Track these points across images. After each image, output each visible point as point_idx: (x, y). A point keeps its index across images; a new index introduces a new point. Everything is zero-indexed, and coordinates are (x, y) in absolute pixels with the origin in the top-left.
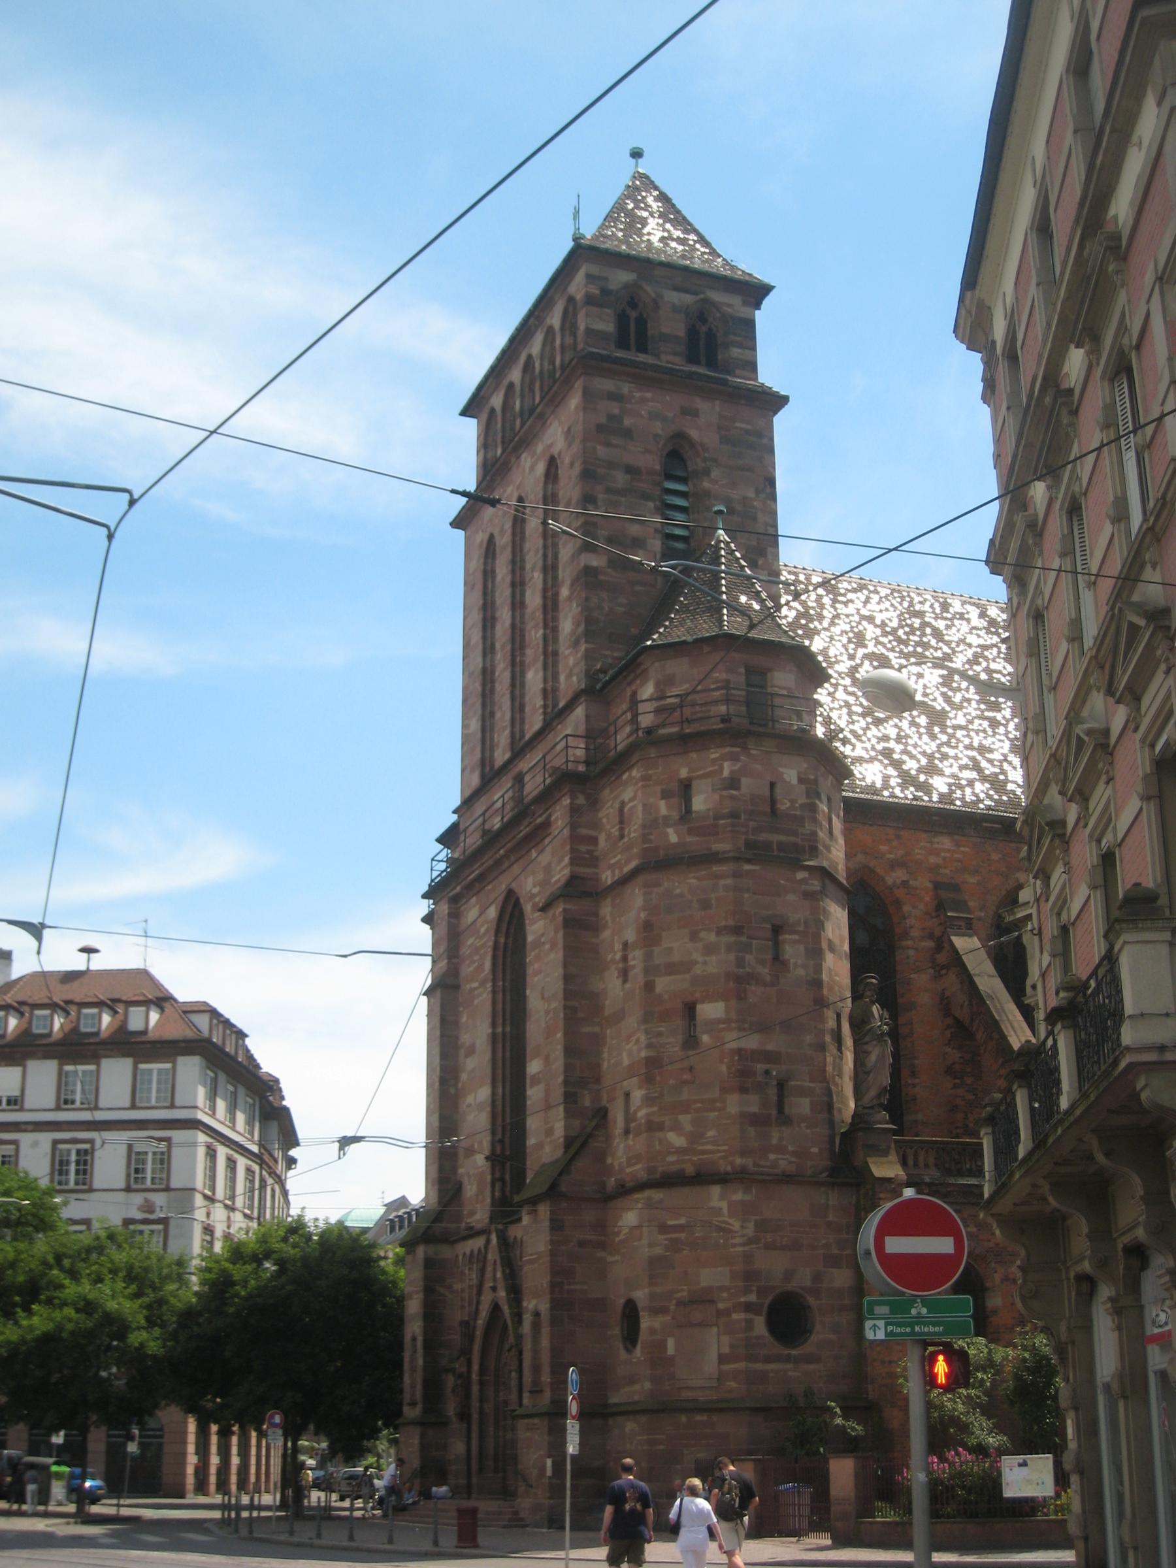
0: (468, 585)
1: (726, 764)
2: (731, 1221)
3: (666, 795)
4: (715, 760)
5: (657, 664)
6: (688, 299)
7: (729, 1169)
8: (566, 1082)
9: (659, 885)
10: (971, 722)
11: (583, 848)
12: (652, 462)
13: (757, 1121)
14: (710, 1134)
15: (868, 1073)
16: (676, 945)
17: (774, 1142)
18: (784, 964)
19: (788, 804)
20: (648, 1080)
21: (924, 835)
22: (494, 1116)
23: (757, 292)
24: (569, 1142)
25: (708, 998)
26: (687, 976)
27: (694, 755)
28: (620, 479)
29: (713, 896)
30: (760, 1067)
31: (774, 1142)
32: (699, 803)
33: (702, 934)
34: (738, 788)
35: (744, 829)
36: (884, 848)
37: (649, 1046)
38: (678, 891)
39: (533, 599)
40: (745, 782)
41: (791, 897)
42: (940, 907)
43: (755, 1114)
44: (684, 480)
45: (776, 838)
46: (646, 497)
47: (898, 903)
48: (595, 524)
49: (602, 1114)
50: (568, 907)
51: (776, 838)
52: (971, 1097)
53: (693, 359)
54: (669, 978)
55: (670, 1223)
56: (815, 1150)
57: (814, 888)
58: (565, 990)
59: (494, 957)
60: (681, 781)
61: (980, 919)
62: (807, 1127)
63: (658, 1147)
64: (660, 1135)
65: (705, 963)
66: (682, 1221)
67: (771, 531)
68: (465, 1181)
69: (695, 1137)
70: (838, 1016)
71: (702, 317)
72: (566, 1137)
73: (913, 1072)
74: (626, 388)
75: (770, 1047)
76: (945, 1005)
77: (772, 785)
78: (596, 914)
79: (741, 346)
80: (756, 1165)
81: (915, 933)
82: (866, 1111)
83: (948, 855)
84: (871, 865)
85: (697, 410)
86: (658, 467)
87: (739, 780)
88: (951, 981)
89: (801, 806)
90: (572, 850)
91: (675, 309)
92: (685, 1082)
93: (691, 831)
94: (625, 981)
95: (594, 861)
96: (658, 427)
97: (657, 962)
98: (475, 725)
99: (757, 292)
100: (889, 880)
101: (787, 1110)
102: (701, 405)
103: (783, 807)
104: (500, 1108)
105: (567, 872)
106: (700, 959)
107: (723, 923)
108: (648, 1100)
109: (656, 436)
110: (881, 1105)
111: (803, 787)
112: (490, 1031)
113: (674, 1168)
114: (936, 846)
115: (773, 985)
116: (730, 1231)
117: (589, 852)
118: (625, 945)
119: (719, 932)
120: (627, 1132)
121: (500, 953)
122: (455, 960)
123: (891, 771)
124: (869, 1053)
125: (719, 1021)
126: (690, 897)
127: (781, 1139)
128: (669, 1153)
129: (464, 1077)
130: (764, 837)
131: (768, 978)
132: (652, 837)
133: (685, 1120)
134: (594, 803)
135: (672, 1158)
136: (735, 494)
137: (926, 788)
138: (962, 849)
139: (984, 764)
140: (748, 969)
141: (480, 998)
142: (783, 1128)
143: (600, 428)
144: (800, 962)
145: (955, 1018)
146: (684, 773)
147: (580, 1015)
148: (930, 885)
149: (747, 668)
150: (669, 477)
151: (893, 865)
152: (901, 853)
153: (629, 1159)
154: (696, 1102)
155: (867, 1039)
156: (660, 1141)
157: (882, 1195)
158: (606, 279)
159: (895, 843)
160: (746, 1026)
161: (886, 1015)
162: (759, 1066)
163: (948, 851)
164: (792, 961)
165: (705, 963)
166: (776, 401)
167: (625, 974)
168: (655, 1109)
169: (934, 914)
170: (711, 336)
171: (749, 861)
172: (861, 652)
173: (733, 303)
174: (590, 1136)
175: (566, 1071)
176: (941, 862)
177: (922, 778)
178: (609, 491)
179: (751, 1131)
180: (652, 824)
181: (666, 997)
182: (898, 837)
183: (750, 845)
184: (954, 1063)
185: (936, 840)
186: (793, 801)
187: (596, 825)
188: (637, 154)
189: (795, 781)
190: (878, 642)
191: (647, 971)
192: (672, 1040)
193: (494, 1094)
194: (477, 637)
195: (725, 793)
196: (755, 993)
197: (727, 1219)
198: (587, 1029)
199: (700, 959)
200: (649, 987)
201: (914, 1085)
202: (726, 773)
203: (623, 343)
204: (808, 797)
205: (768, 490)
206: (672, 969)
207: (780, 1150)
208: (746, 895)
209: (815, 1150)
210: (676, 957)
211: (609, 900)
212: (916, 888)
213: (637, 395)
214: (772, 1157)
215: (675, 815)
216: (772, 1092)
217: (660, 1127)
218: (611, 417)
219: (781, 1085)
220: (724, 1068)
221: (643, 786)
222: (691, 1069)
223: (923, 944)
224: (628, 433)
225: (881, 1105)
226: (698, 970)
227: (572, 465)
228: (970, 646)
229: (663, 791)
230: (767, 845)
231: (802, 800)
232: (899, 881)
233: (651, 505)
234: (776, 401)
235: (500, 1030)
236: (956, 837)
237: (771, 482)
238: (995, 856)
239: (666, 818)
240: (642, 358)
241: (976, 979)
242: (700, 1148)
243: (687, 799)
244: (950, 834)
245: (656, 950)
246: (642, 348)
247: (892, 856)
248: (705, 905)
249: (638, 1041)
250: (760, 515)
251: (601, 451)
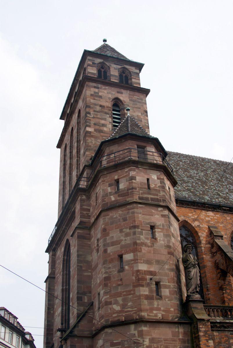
0: (61, 161)
1: (130, 172)
2: (139, 339)
3: (110, 185)
4: (126, 172)
5: (107, 148)
6: (120, 67)
7: (137, 317)
8: (78, 293)
9: (108, 215)
10: (215, 185)
11: (85, 213)
12: (109, 104)
13: (148, 297)
14: (129, 304)
15: (191, 279)
16: (115, 235)
17: (155, 306)
18: (156, 239)
19: (154, 186)
20: (106, 285)
21: (203, 211)
22: (62, 317)
23: (140, 66)
24: (78, 315)
25: (127, 252)
26: (119, 245)
27: (120, 171)
28: (98, 108)
29: (128, 216)
30: (148, 277)
31: (155, 306)
32: (122, 186)
33: (124, 230)
34: (136, 180)
35: (138, 193)
36: (190, 215)
37: (106, 273)
38: (115, 216)
39: (75, 151)
40: (138, 178)
41: (157, 216)
42: (211, 233)
43: (147, 295)
44: (119, 111)
45: (150, 196)
46: (106, 113)
47: (196, 233)
48: (90, 120)
49: (92, 304)
50: (79, 231)
51: (150, 196)
52: (229, 297)
54: (112, 247)
55: (115, 342)
56: (172, 309)
57: (165, 214)
58: (78, 260)
59: (63, 263)
60: (115, 180)
61: (225, 238)
62: (169, 300)
63: (109, 311)
64: (110, 306)
65: (126, 240)
66: (120, 340)
67: (147, 124)
68: (55, 343)
69: (124, 306)
70: (178, 261)
72: (77, 313)
73: (208, 290)
74: (100, 86)
75: (152, 269)
76: (216, 265)
77: (148, 180)
78: (90, 234)
79: (135, 79)
80: (148, 315)
81: (204, 242)
82: (191, 294)
83: (212, 217)
84: (187, 220)
85: (122, 92)
86: (110, 106)
87: (136, 177)
88: (218, 257)
89: (159, 186)
90: (81, 213)
91: (115, 69)
92: (119, 285)
93: (119, 196)
94: (98, 253)
95: (89, 217)
96: (110, 96)
97: (108, 242)
98: (61, 198)
99: (140, 66)
100: (193, 225)
101: (159, 294)
103: (152, 187)
104: (64, 315)
105: (79, 221)
106: (124, 239)
107: (132, 225)
108: (105, 293)
109: (109, 98)
110: (197, 292)
111: (159, 181)
112: (62, 288)
113: (116, 319)
114: (208, 214)
115: (152, 247)
116: (139, 343)
117: (86, 214)
118: (98, 240)
119: (130, 229)
120: (99, 308)
121: (65, 262)
122: (54, 269)
123: (191, 194)
124: (191, 272)
125: (132, 260)
126: (119, 218)
127: (158, 305)
128: (115, 313)
129: (55, 306)
130: (145, 196)
131: (150, 244)
132: (105, 200)
133: (120, 299)
134: (89, 198)
135: (114, 315)
137: (203, 198)
138: (217, 216)
139: (221, 194)
140: (141, 241)
141: (59, 278)
142: (159, 301)
143: (92, 95)
144: (161, 239)
145: (221, 270)
146: (116, 177)
147: (83, 269)
148: (207, 227)
149: (137, 145)
150: (114, 110)
151: (195, 220)
152: (196, 216)
153: (100, 318)
154: (123, 292)
155: (189, 266)
156: (110, 309)
157: (201, 326)
158: (94, 60)
159: (194, 213)
160: (142, 261)
161: (196, 258)
162: (147, 276)
163: (212, 216)
164: (158, 238)
165: (126, 240)
166: (146, 92)
167: (98, 251)
168: (108, 296)
169: (209, 236)
170: (126, 77)
171: (140, 203)
172: (178, 167)
173: (133, 69)
174: (86, 312)
175: (78, 289)
176: (210, 220)
177: (201, 196)
178: (94, 111)
179: (146, 302)
180: (106, 195)
181: (111, 254)
182: (195, 211)
183: (140, 198)
184: (222, 285)
185: (208, 213)
186: (156, 185)
187: (89, 205)
188: (105, 41)
189: (156, 178)
190: (183, 166)
191: (104, 245)
192: (114, 269)
193: (62, 309)
194: (62, 174)
195: (131, 181)
196: (144, 249)
197: (137, 338)
198: (86, 274)
199: (124, 239)
200: (105, 251)
201: (208, 294)
202: (131, 175)
204: (161, 183)
205: (145, 114)
206: (113, 244)
207: (158, 309)
208: (140, 215)
209: (172, 309)
210: (115, 239)
211: (93, 228)
212: (202, 228)
213: (104, 87)
214: (155, 312)
215: (114, 191)
216: (154, 287)
217: (110, 303)
218: (95, 92)
219: (157, 284)
220: (134, 278)
221: (103, 184)
222: (121, 280)
223: (207, 246)
224: (101, 97)
225: (197, 292)
226: (123, 243)
227: (84, 107)
228: (212, 168)
229: (109, 184)
230: (147, 199)
231: (159, 185)
232: (196, 225)
233: (108, 115)
234: (146, 92)
235: (65, 287)
236: (215, 212)
237: (146, 112)
238: (228, 218)
239: (110, 193)
241: (227, 253)
242: (126, 310)
243: (118, 187)
244: (212, 211)
245: (108, 238)
247: (193, 217)
248: (125, 220)
249: (102, 272)
250: (143, 120)
251: (92, 101)
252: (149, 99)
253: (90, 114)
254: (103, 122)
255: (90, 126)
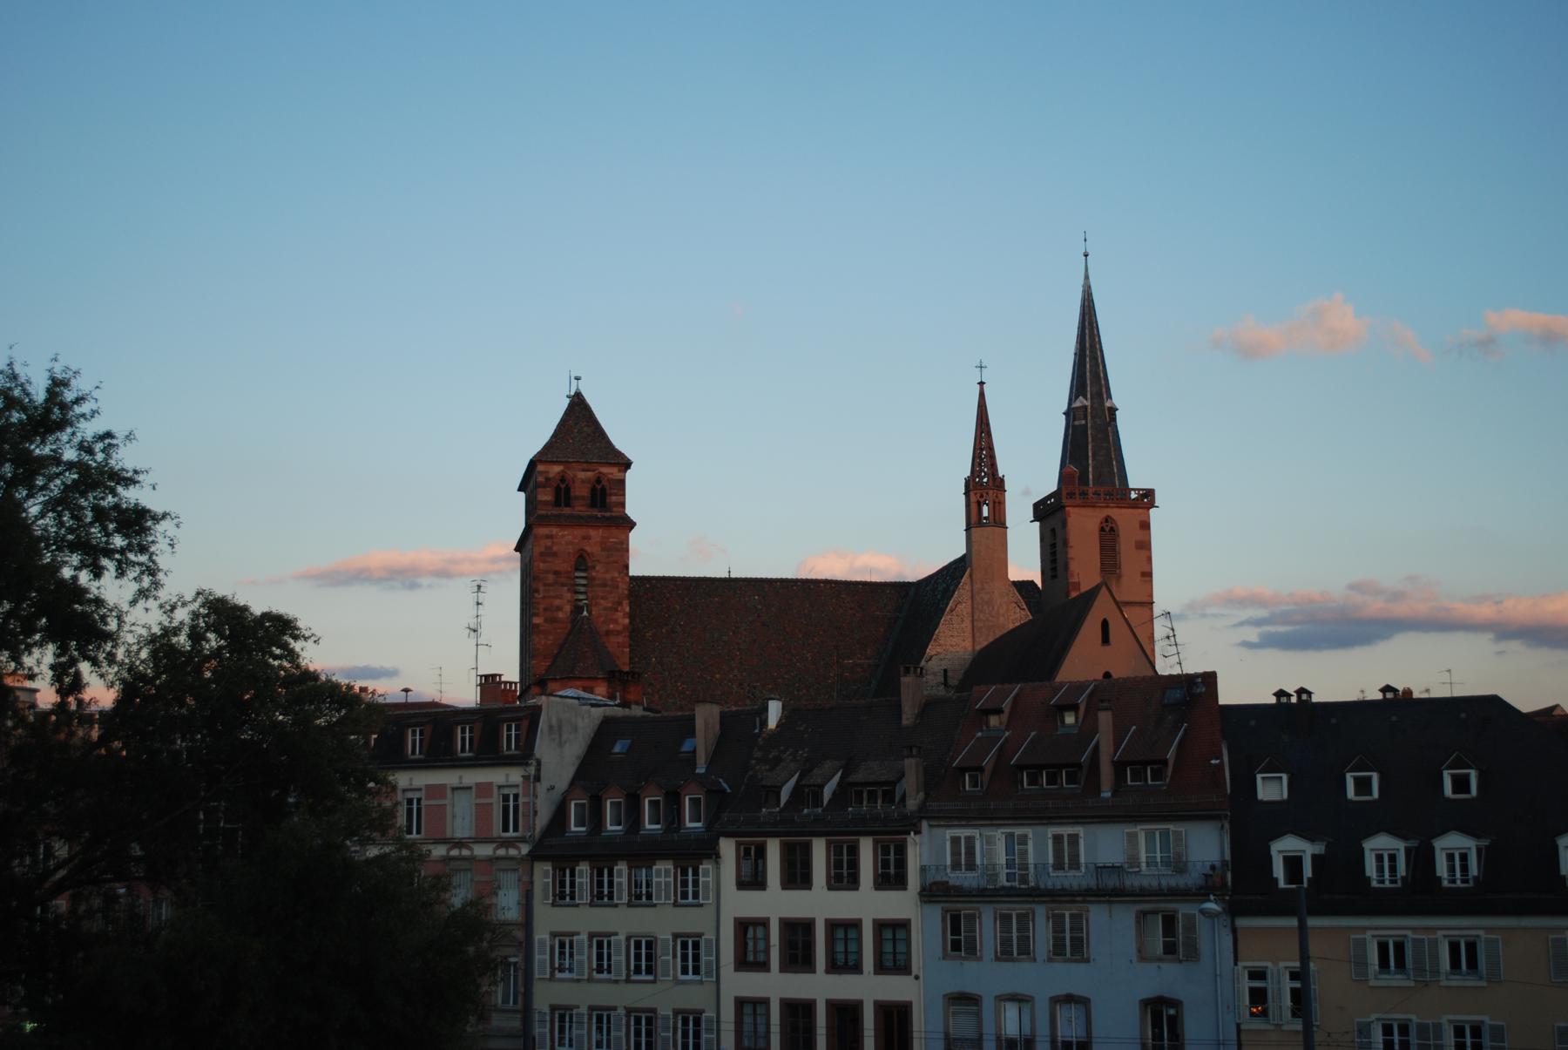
23: (627, 464)
28: (551, 578)
44: (585, 570)
53: (593, 504)
71: (598, 481)
74: (555, 531)
91: (583, 481)
102: (592, 533)
136: (608, 576)
143: (541, 554)
150: (577, 569)
166: (631, 525)
170: (603, 489)
188: (578, 379)
203: (557, 503)
218: (548, 548)
224: (555, 554)
240: (567, 511)
246: (567, 505)
252: (633, 536)
253: (537, 591)
254: (557, 602)
255: (536, 615)
